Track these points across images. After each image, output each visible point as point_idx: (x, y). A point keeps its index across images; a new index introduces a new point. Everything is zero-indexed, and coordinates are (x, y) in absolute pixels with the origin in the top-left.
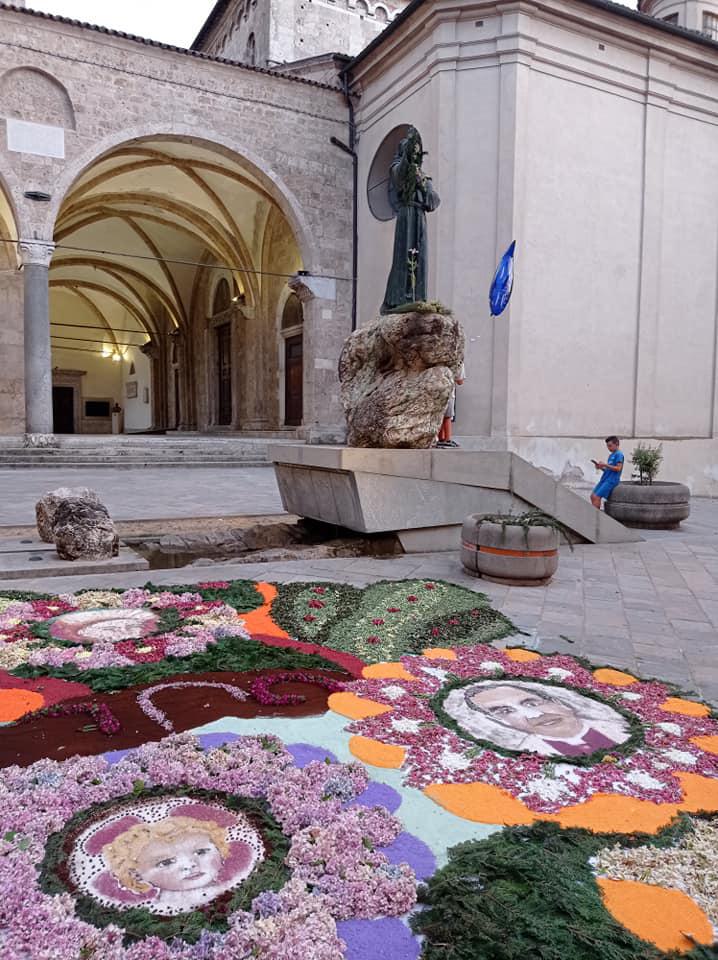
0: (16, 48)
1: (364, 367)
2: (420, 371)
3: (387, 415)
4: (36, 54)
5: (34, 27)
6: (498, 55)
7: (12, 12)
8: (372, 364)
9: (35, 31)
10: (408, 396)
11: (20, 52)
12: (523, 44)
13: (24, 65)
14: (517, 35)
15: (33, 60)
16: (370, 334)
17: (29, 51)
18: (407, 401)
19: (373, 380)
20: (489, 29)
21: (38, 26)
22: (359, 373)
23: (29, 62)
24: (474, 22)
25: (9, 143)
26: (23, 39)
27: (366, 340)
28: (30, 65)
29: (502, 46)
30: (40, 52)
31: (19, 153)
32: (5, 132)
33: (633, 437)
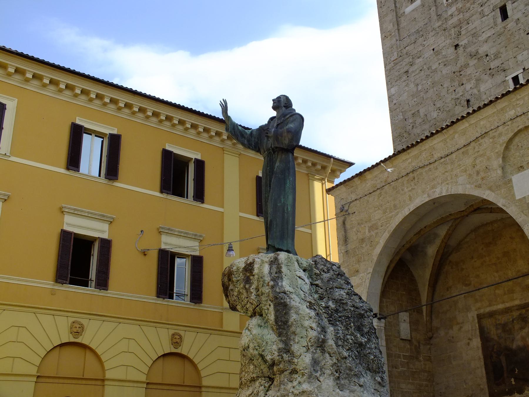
0: (509, 123)
4: (523, 116)
5: (518, 100)
7: (499, 101)
9: (518, 102)
11: (512, 124)
13: (516, 131)
15: (520, 124)
17: (518, 119)
21: (519, 97)
23: (518, 126)
25: (516, 194)
26: (512, 113)
28: (520, 127)
30: (524, 113)
31: (524, 198)
32: (513, 188)
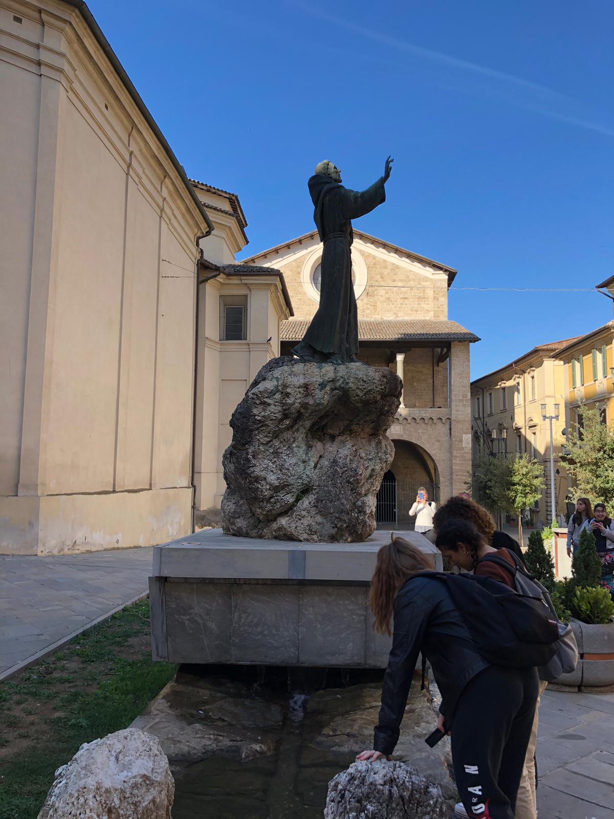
1: (297, 426)
2: (370, 441)
3: (360, 494)
6: (39, 64)
8: (308, 424)
10: (373, 470)
12: (66, 68)
14: (63, 55)
16: (322, 386)
18: (371, 476)
19: (309, 447)
20: (28, 30)
22: (288, 435)
24: (12, 15)
27: (319, 394)
29: (45, 56)
33: (114, 492)
